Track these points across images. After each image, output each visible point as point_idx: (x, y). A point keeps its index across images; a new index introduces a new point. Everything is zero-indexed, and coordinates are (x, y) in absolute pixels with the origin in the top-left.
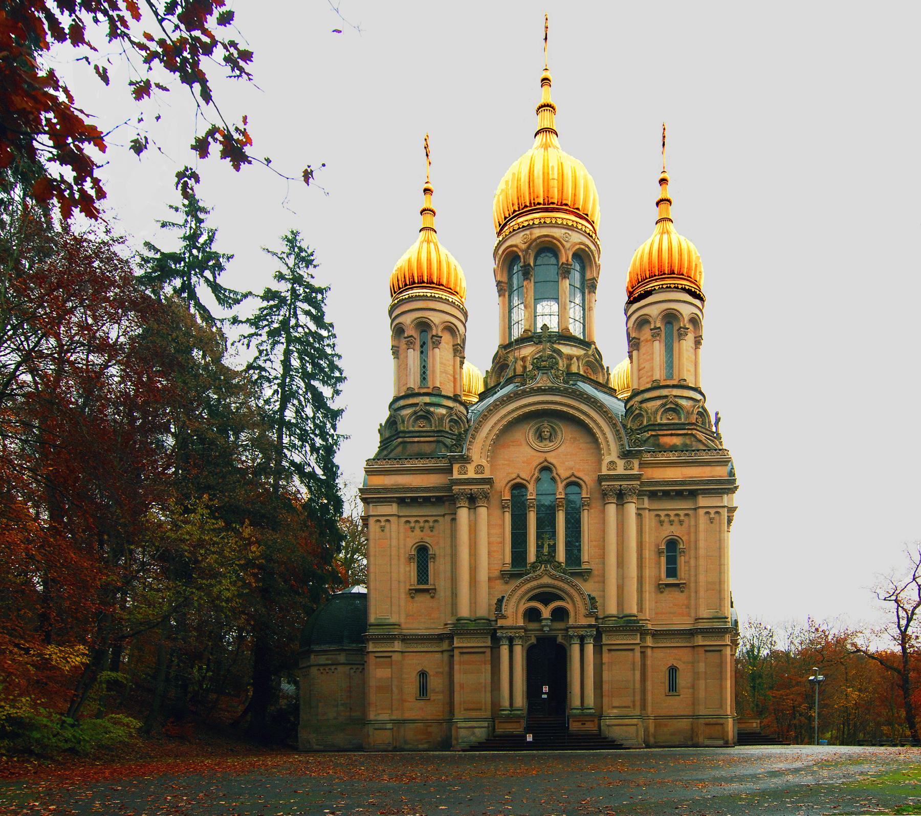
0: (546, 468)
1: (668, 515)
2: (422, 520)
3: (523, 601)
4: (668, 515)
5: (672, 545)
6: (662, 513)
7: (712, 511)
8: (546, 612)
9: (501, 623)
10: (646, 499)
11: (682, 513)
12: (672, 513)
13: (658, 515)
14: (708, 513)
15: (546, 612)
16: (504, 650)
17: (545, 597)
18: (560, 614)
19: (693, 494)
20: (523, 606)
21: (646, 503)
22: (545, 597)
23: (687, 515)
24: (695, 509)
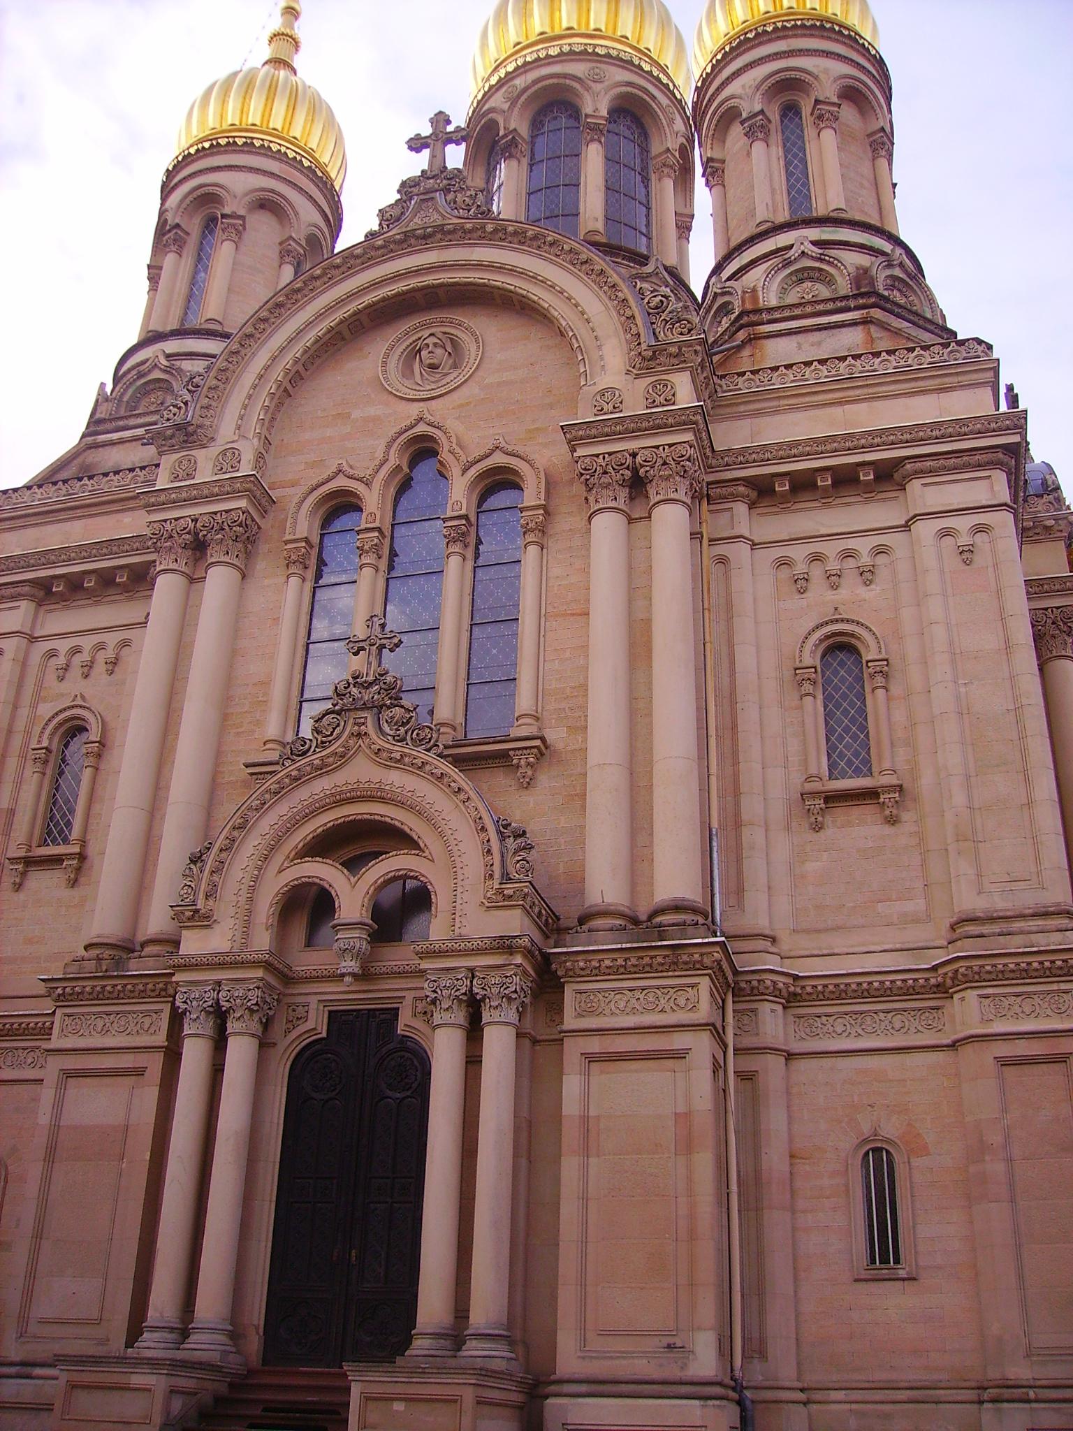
0: (423, 450)
1: (817, 558)
2: (87, 643)
3: (279, 859)
4: (817, 558)
5: (841, 647)
6: (799, 553)
7: (963, 524)
8: (353, 896)
9: (193, 944)
10: (741, 509)
11: (863, 546)
12: (831, 549)
13: (784, 562)
14: (946, 533)
15: (353, 896)
16: (195, 1054)
17: (355, 841)
18: (402, 909)
19: (889, 477)
20: (275, 884)
21: (740, 517)
22: (355, 841)
23: (881, 550)
24: (906, 527)
